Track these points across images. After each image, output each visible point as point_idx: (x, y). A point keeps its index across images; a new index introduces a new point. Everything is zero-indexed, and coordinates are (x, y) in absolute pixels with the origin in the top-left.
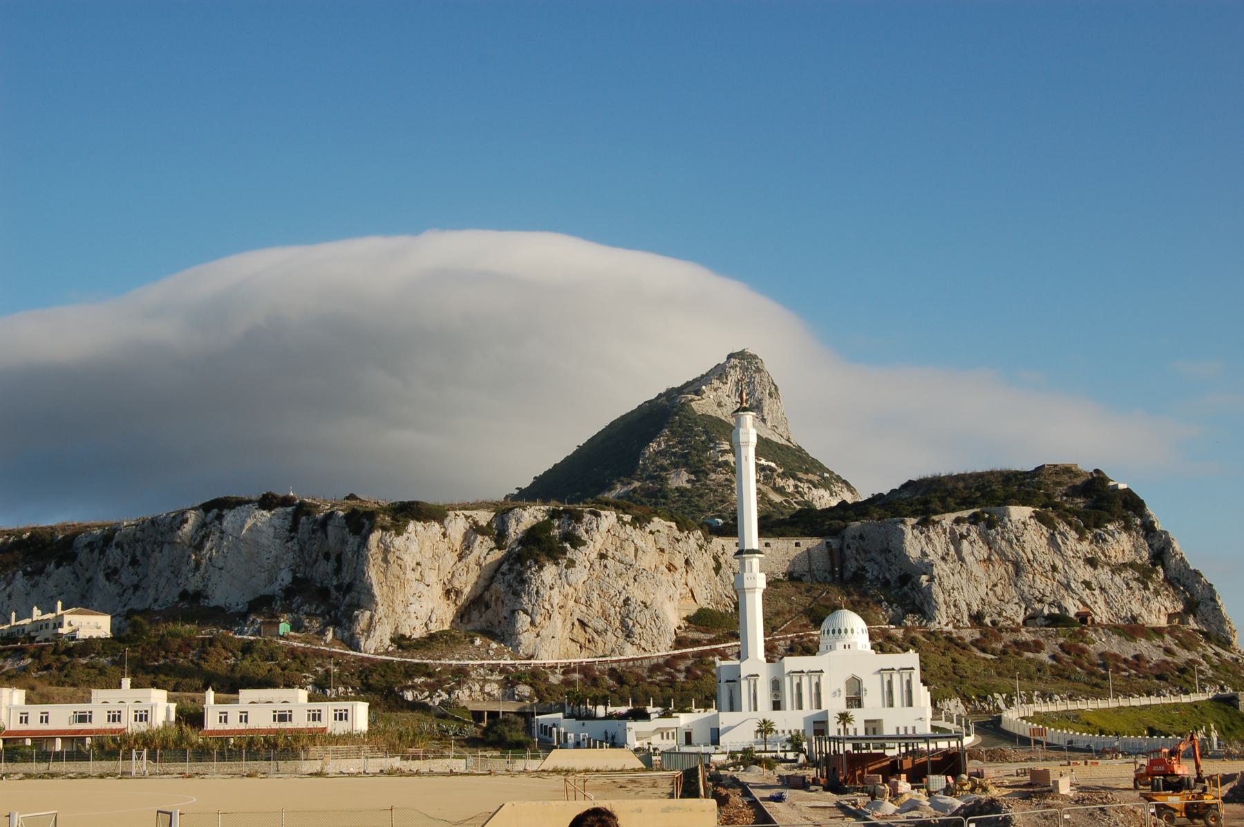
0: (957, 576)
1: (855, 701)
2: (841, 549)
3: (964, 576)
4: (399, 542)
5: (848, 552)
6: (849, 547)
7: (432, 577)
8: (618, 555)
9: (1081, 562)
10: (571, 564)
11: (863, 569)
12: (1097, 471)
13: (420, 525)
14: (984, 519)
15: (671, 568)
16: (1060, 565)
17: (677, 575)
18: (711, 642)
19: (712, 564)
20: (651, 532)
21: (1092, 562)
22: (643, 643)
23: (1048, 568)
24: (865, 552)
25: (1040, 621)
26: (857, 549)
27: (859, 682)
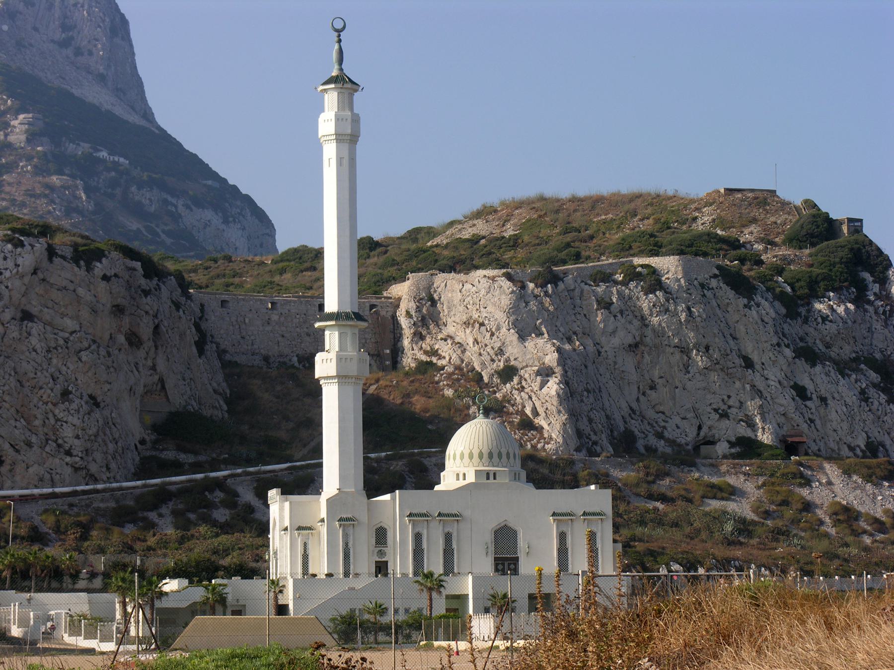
1: (506, 563)
2: (394, 317)
3: (602, 370)
9: (788, 352)
11: (434, 353)
12: (810, 204)
15: (134, 340)
16: (755, 357)
17: (141, 353)
18: (197, 467)
19: (192, 335)
20: (105, 278)
21: (808, 355)
22: (93, 468)
23: (739, 362)
25: (722, 448)
27: (515, 533)
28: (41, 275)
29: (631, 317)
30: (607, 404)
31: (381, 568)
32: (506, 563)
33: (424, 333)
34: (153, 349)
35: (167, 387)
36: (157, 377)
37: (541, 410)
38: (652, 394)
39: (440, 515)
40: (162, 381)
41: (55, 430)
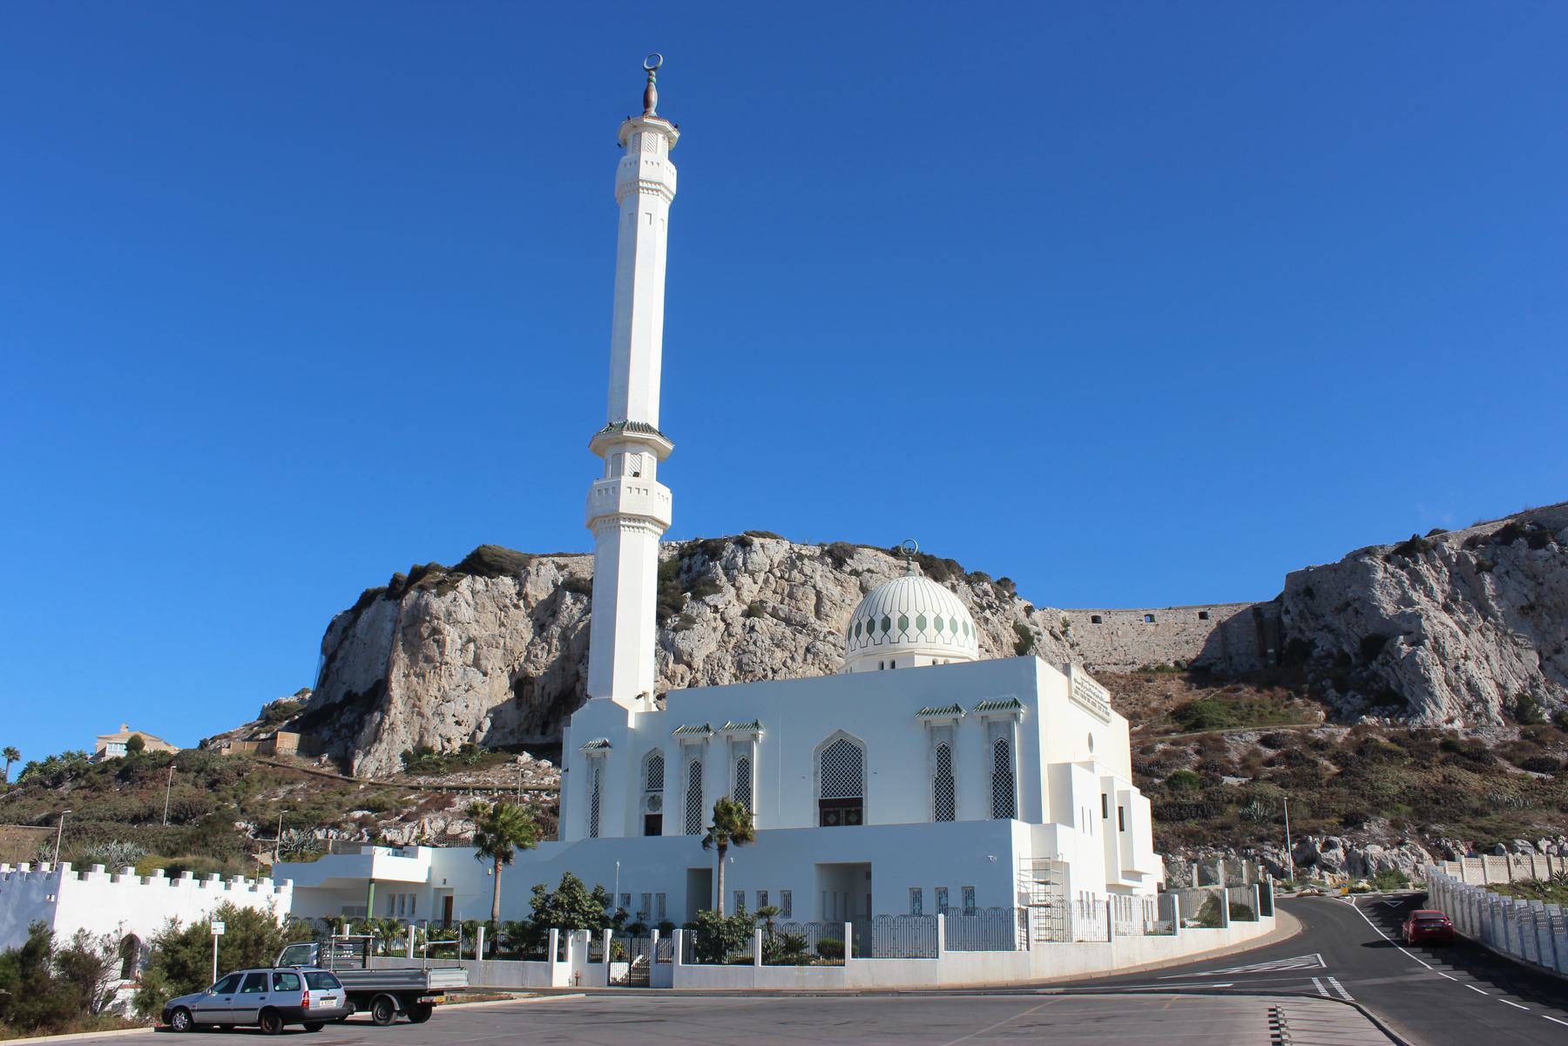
0: (1476, 637)
1: (841, 809)
4: (438, 605)
5: (1286, 619)
6: (1287, 612)
7: (494, 660)
8: (784, 609)
10: (688, 622)
13: (480, 583)
14: (1524, 534)
24: (1317, 617)
26: (1301, 614)
29: (1520, 576)
30: (1497, 671)
31: (653, 826)
32: (841, 809)
33: (1303, 626)
37: (1404, 682)
38: (1556, 657)
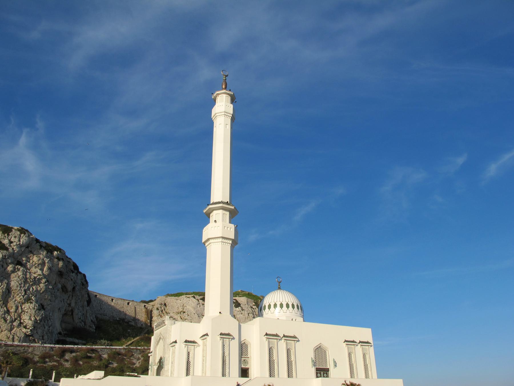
15: (64, 289)
28: (30, 249)
31: (244, 373)
34: (71, 297)
35: (74, 314)
36: (70, 308)
39: (284, 336)
40: (72, 311)
41: (20, 316)
